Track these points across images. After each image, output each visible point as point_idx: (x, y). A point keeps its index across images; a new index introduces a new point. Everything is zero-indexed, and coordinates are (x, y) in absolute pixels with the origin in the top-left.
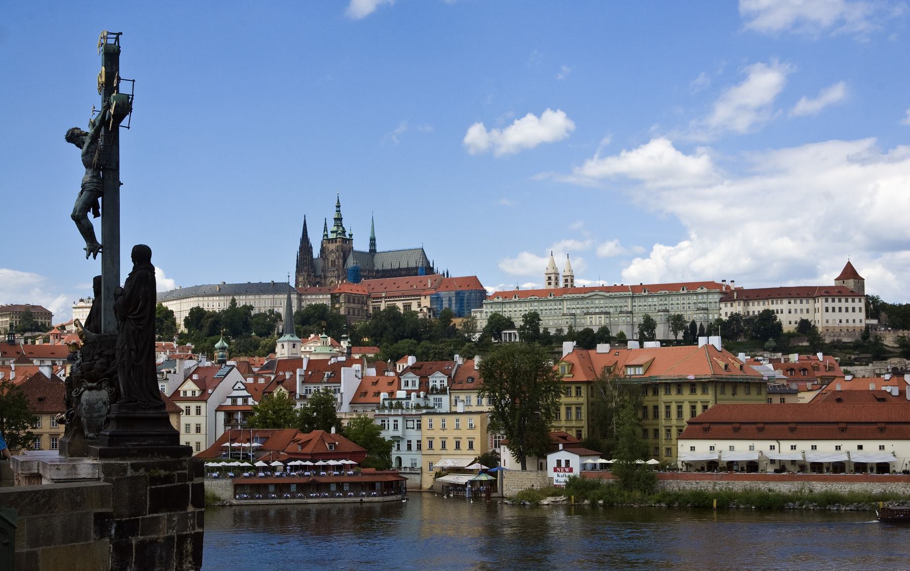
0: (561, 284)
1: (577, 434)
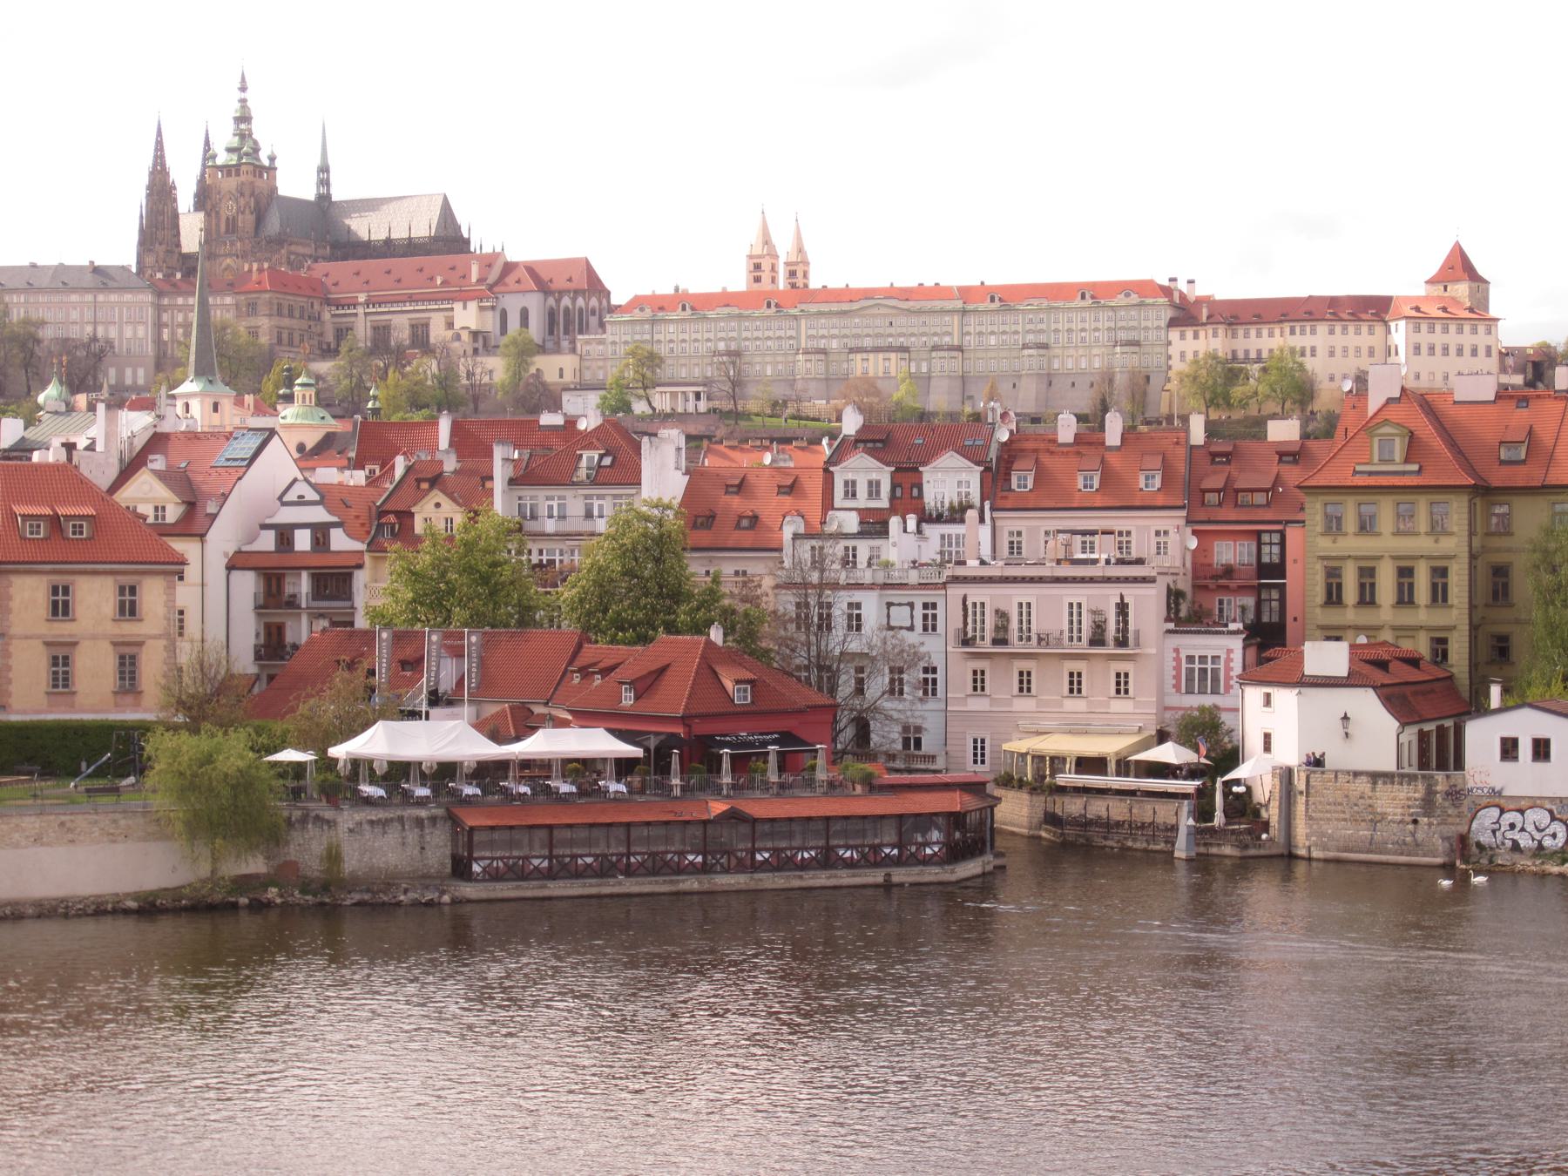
0: (782, 284)
1: (1435, 652)
